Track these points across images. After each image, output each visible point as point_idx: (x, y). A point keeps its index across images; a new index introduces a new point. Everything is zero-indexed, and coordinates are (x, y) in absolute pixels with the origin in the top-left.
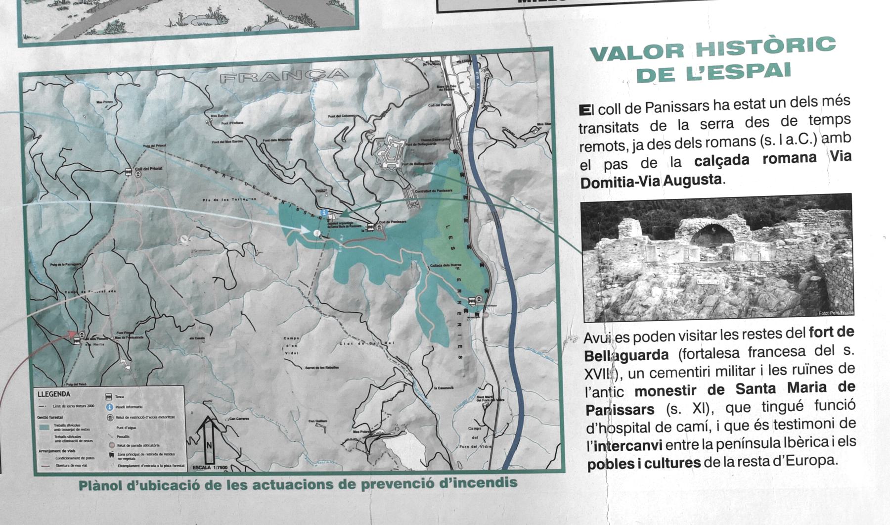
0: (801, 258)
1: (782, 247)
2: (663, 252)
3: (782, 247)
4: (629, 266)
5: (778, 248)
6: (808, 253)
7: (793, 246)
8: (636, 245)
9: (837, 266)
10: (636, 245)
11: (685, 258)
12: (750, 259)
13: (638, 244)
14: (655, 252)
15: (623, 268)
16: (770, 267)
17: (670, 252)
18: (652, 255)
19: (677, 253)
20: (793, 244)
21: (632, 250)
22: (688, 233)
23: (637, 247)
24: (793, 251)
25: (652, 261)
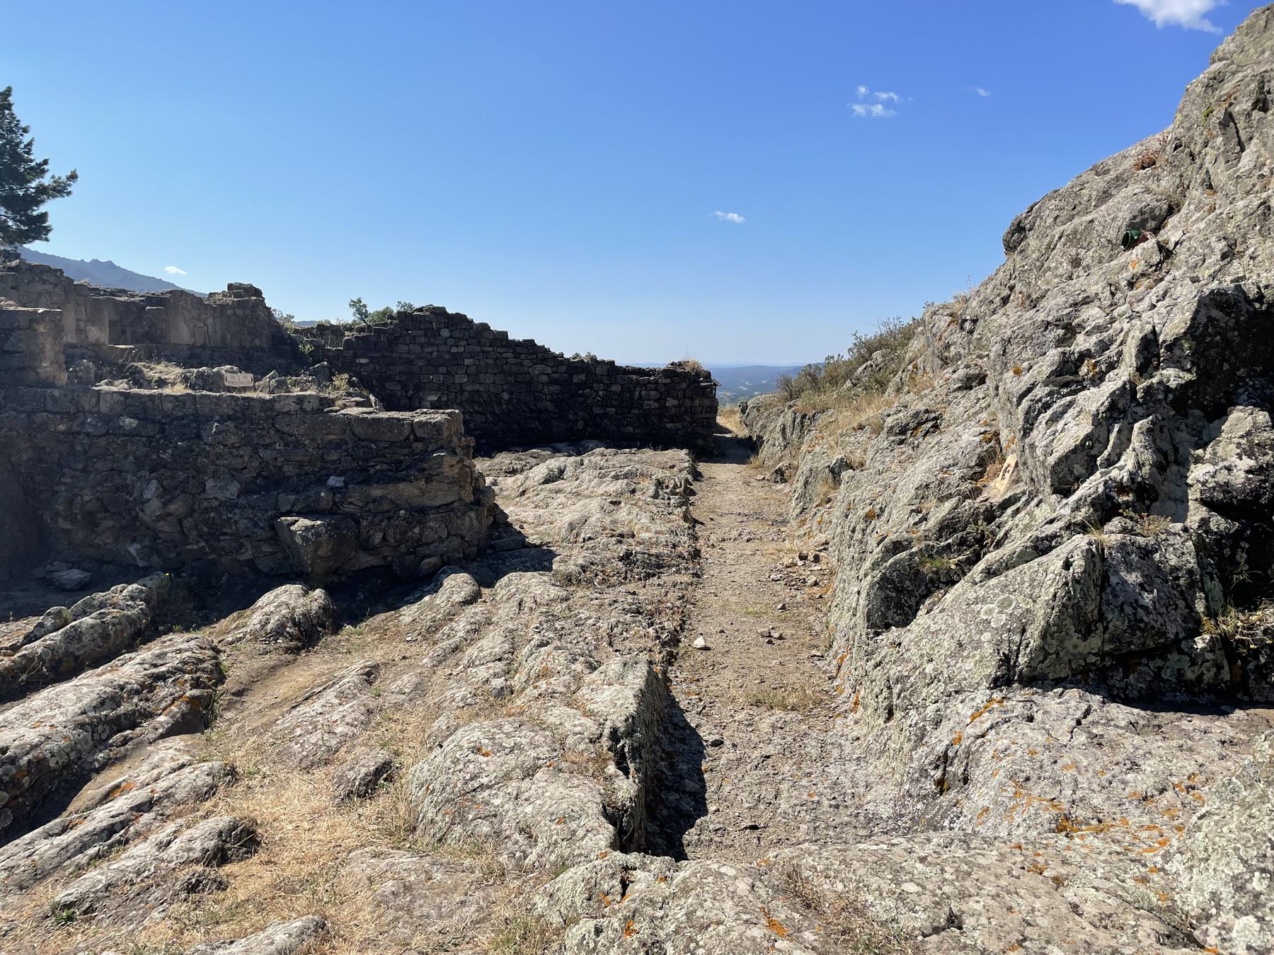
5: (229, 312)
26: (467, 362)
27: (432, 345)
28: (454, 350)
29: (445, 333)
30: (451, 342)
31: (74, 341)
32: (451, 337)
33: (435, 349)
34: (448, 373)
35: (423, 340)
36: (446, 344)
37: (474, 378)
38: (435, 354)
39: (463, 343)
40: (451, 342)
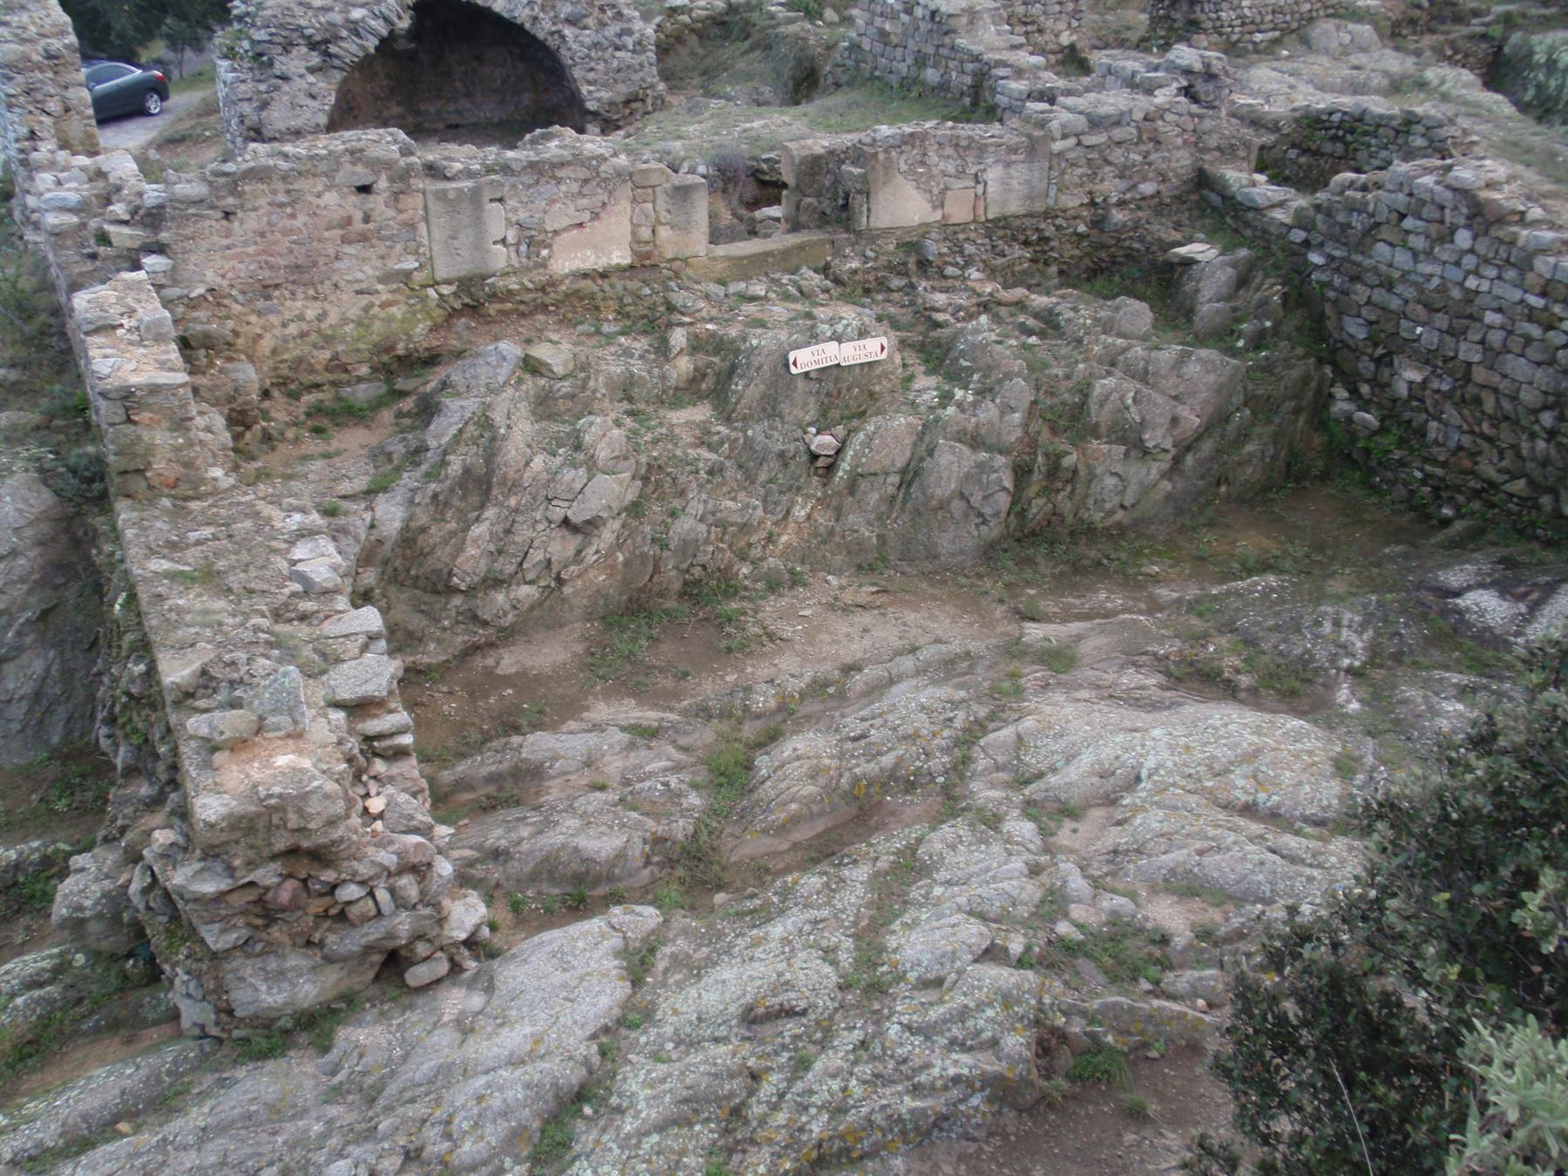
0: (1148, 188)
1: (1072, 141)
2: (522, 215)
3: (1072, 141)
4: (333, 318)
5: (1058, 146)
6: (1181, 161)
7: (1118, 134)
8: (365, 189)
9: (1409, 223)
10: (365, 189)
11: (636, 240)
12: (938, 215)
13: (383, 184)
14: (478, 222)
15: (293, 329)
16: (1026, 243)
17: (559, 217)
18: (466, 238)
19: (596, 216)
20: (1118, 124)
21: (348, 221)
22: (315, 59)
23: (377, 202)
24: (1117, 155)
25: (463, 273)
26: (1491, 317)
27: (1435, 260)
28: (1472, 283)
29: (1463, 238)
30: (1469, 262)
31: (627, 261)
32: (1472, 251)
33: (1437, 269)
34: (1451, 332)
35: (1418, 242)
36: (1458, 264)
37: (1492, 356)
38: (1436, 282)
39: (1491, 272)
40: (1469, 262)
